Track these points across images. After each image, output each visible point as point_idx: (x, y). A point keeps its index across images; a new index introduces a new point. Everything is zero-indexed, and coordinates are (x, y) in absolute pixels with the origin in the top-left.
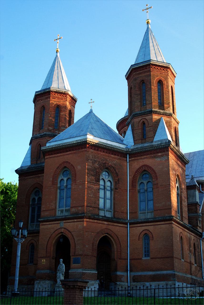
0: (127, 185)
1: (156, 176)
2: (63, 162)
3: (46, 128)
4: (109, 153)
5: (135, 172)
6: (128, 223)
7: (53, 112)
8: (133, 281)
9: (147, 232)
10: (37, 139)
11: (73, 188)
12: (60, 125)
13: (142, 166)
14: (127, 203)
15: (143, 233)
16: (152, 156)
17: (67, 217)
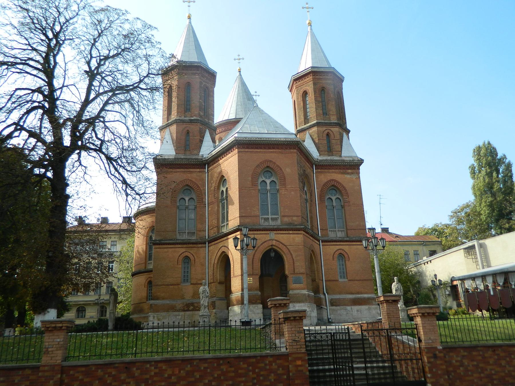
1: (347, 193)
9: (343, 252)
10: (183, 122)
11: (283, 193)
15: (337, 253)
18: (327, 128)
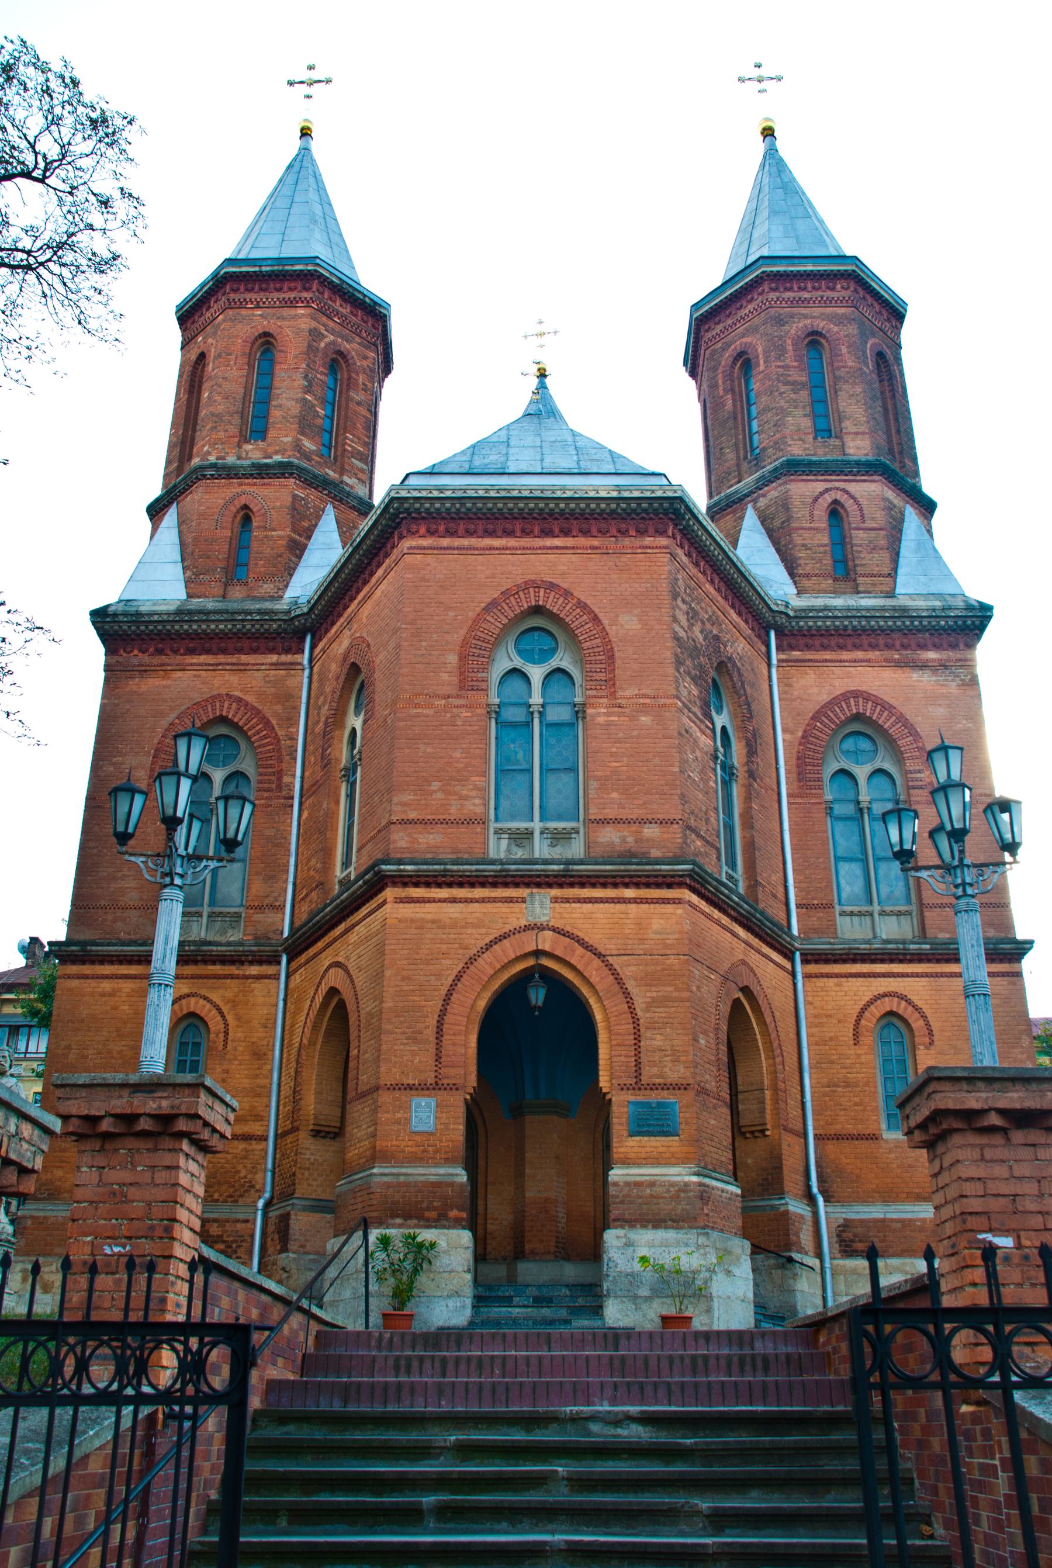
0: (774, 770)
2: (526, 583)
3: (285, 440)
4: (726, 598)
5: (812, 718)
6: (798, 954)
7: (318, 376)
8: (840, 1251)
9: (902, 1008)
10: (229, 477)
11: (601, 720)
12: (349, 445)
13: (846, 696)
14: (781, 858)
15: (876, 1011)
16: (897, 657)
17: (576, 867)
18: (829, 485)
